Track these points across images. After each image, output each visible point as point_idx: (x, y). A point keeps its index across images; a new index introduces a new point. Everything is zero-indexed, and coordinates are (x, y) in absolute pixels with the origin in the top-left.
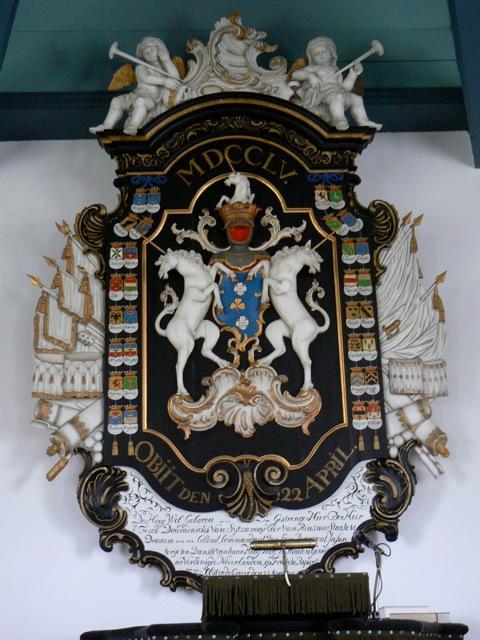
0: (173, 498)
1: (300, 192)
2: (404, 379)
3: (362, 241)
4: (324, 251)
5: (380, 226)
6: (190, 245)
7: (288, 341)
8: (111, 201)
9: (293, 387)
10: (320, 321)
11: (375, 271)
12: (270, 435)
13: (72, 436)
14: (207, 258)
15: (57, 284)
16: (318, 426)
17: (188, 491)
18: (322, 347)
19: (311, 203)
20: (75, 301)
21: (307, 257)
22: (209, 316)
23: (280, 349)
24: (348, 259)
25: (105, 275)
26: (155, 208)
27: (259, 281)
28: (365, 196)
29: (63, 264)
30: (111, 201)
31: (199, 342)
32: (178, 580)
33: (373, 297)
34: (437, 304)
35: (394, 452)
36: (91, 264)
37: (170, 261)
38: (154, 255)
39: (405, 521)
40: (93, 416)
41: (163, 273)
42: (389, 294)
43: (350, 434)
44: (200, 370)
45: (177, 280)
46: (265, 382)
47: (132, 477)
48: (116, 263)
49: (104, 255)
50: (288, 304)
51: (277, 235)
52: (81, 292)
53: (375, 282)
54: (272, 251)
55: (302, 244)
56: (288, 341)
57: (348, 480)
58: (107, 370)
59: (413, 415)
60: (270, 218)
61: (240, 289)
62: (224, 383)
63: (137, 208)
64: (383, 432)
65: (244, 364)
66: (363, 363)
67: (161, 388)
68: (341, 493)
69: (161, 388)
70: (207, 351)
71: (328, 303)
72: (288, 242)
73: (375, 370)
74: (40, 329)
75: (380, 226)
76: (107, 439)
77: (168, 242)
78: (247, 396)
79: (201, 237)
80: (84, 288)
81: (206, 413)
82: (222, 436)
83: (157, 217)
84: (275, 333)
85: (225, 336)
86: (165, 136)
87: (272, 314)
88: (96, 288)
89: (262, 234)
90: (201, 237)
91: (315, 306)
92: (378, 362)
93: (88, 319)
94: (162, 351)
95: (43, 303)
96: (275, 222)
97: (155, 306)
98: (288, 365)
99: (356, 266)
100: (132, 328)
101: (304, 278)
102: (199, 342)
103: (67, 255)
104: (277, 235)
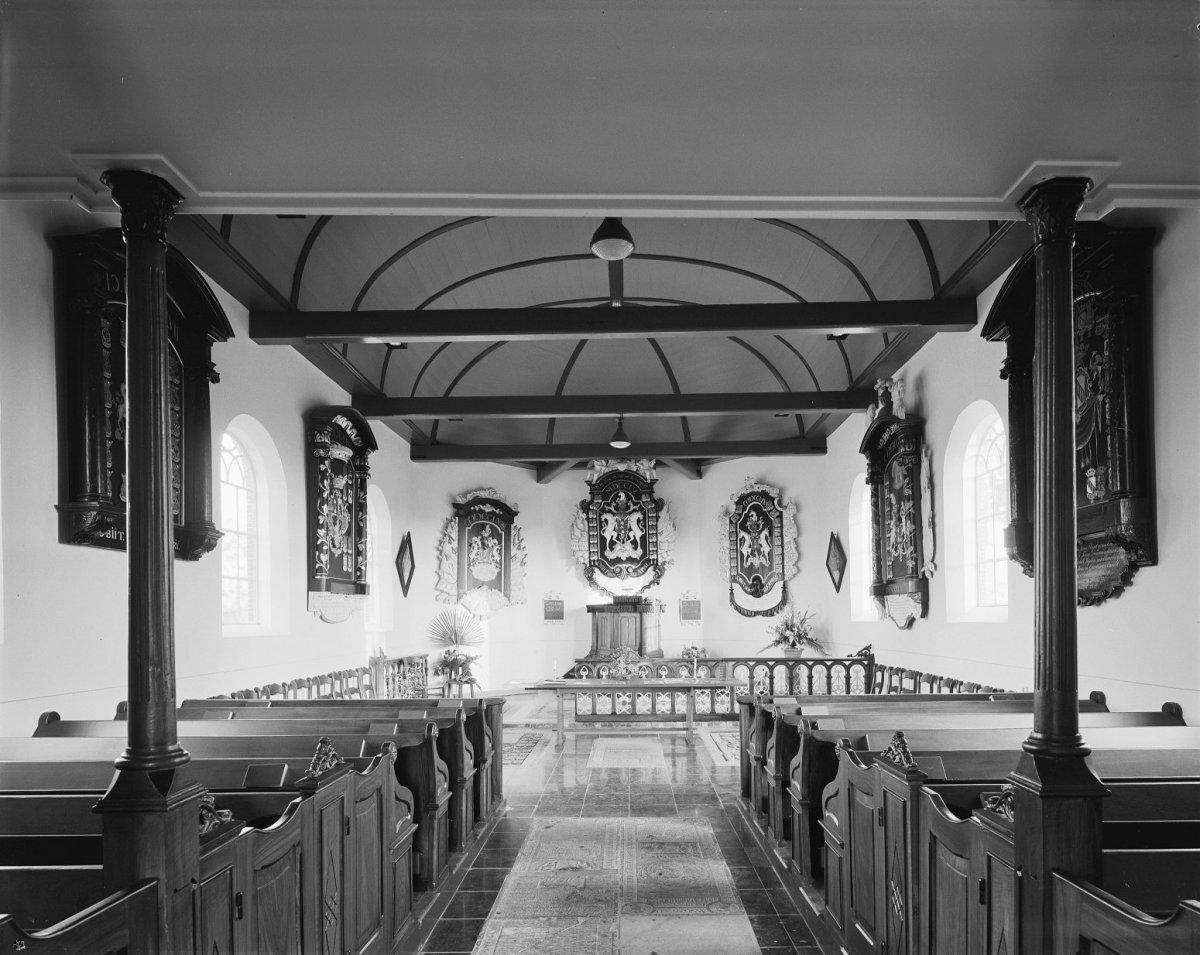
1: (638, 497)
2: (663, 547)
4: (644, 514)
5: (659, 505)
6: (610, 511)
8: (588, 498)
9: (636, 548)
10: (642, 530)
11: (657, 518)
12: (630, 560)
13: (582, 561)
14: (614, 515)
18: (643, 538)
19: (641, 499)
20: (581, 526)
21: (639, 515)
23: (632, 538)
25: (588, 519)
26: (600, 501)
28: (656, 496)
30: (588, 498)
32: (609, 594)
34: (674, 526)
36: (584, 516)
37: (604, 516)
38: (600, 515)
39: (662, 580)
40: (587, 555)
43: (649, 560)
44: (612, 543)
45: (606, 520)
46: (628, 546)
48: (591, 516)
49: (588, 514)
50: (634, 527)
51: (632, 508)
52: (582, 525)
53: (657, 521)
54: (631, 513)
58: (589, 544)
59: (665, 555)
60: (630, 503)
62: (618, 547)
63: (596, 501)
65: (623, 542)
67: (603, 549)
69: (603, 549)
70: (614, 539)
71: (645, 526)
72: (635, 510)
73: (656, 544)
75: (659, 505)
76: (590, 561)
77: (604, 511)
79: (612, 509)
80: (583, 522)
82: (618, 560)
84: (631, 534)
85: (619, 535)
86: (602, 481)
87: (630, 529)
88: (586, 522)
89: (628, 508)
90: (612, 509)
94: (603, 539)
97: (601, 527)
98: (634, 542)
101: (638, 520)
104: (632, 508)
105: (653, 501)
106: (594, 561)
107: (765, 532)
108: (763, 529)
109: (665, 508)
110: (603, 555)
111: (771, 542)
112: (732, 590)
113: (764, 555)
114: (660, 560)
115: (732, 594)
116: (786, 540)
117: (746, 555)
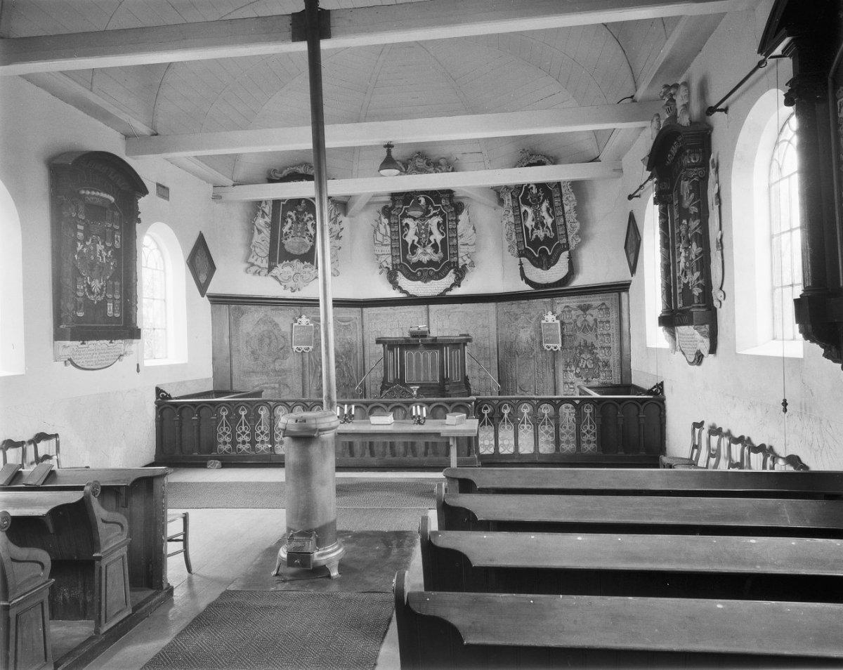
0: (408, 278)
3: (454, 214)
4: (444, 217)
7: (435, 240)
9: (436, 252)
10: (442, 234)
11: (457, 221)
12: (431, 263)
13: (385, 265)
15: (378, 226)
16: (443, 260)
17: (412, 277)
18: (444, 241)
19: (441, 204)
20: (383, 231)
22: (416, 234)
23: (433, 242)
24: (450, 219)
25: (390, 224)
26: (401, 206)
27: (428, 225)
29: (379, 221)
31: (413, 241)
33: (456, 228)
34: (474, 229)
35: (460, 267)
36: (386, 221)
37: (406, 221)
38: (401, 220)
40: (389, 260)
41: (404, 225)
42: (461, 227)
44: (414, 247)
45: (407, 225)
46: (429, 250)
47: (399, 273)
51: (433, 212)
53: (457, 224)
54: (431, 217)
55: (438, 215)
56: (435, 240)
57: (449, 274)
59: (465, 258)
61: (423, 227)
62: (420, 251)
63: (397, 206)
64: (457, 262)
65: (424, 246)
66: (453, 245)
67: (405, 253)
68: (447, 276)
69: (405, 253)
70: (415, 243)
71: (445, 230)
72: (435, 215)
74: (375, 238)
76: (393, 265)
77: (405, 216)
78: (425, 254)
80: (385, 227)
81: (415, 258)
82: (420, 263)
83: (402, 209)
84: (432, 238)
85: (419, 239)
87: (431, 233)
91: (442, 231)
92: (457, 245)
93: (386, 235)
94: (405, 243)
95: (375, 232)
96: (432, 209)
97: (403, 232)
98: (435, 246)
99: (452, 220)
100: (397, 238)
101: (439, 224)
102: (413, 241)
103: (380, 218)
104: (433, 212)
105: (453, 204)
106: (396, 265)
107: (545, 205)
108: (543, 201)
109: (465, 212)
110: (405, 259)
111: (553, 213)
112: (521, 264)
113: (547, 227)
114: (461, 263)
115: (522, 269)
116: (567, 208)
117: (530, 228)
